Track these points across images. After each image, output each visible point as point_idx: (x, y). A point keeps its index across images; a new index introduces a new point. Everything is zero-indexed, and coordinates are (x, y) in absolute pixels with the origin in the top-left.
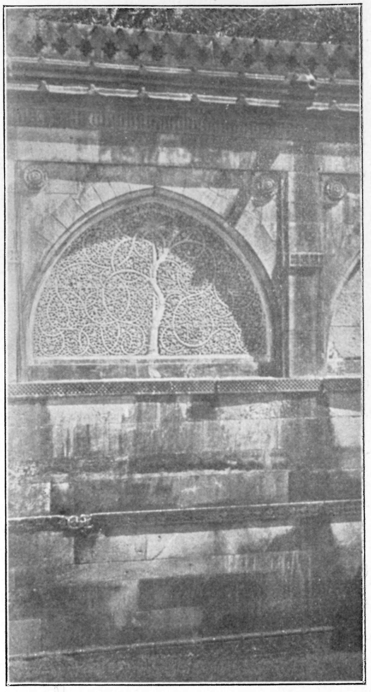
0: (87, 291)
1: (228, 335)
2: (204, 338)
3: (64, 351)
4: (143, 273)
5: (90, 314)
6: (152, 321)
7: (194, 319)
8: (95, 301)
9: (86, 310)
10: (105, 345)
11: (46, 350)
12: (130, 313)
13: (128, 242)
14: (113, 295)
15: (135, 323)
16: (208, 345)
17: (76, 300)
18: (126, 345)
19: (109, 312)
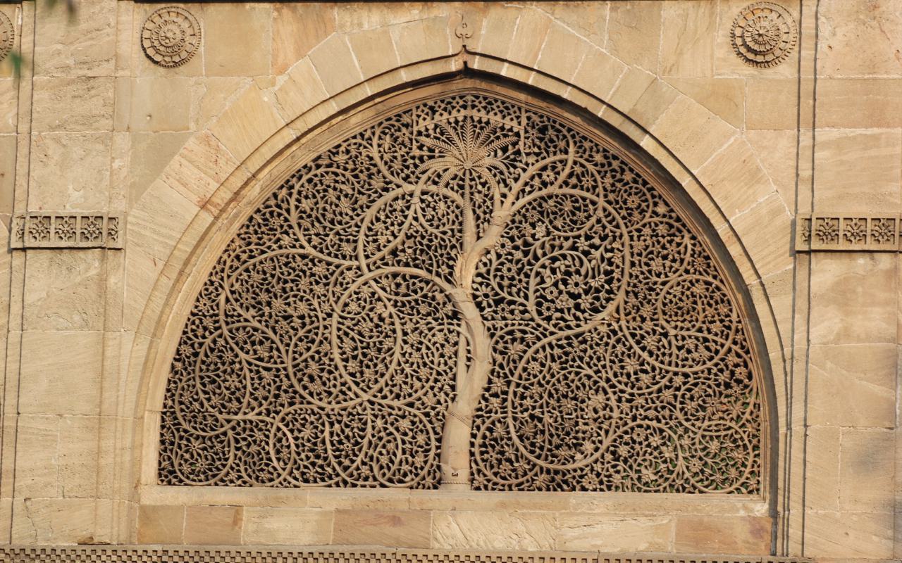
0: (297, 322)
1: (656, 440)
2: (588, 447)
3: (233, 475)
4: (438, 275)
5: (300, 380)
6: (453, 399)
8: (314, 348)
9: (291, 370)
10: (334, 461)
11: (186, 468)
12: (399, 379)
14: (360, 334)
15: (411, 405)
16: (598, 467)
17: (267, 344)
19: (348, 378)
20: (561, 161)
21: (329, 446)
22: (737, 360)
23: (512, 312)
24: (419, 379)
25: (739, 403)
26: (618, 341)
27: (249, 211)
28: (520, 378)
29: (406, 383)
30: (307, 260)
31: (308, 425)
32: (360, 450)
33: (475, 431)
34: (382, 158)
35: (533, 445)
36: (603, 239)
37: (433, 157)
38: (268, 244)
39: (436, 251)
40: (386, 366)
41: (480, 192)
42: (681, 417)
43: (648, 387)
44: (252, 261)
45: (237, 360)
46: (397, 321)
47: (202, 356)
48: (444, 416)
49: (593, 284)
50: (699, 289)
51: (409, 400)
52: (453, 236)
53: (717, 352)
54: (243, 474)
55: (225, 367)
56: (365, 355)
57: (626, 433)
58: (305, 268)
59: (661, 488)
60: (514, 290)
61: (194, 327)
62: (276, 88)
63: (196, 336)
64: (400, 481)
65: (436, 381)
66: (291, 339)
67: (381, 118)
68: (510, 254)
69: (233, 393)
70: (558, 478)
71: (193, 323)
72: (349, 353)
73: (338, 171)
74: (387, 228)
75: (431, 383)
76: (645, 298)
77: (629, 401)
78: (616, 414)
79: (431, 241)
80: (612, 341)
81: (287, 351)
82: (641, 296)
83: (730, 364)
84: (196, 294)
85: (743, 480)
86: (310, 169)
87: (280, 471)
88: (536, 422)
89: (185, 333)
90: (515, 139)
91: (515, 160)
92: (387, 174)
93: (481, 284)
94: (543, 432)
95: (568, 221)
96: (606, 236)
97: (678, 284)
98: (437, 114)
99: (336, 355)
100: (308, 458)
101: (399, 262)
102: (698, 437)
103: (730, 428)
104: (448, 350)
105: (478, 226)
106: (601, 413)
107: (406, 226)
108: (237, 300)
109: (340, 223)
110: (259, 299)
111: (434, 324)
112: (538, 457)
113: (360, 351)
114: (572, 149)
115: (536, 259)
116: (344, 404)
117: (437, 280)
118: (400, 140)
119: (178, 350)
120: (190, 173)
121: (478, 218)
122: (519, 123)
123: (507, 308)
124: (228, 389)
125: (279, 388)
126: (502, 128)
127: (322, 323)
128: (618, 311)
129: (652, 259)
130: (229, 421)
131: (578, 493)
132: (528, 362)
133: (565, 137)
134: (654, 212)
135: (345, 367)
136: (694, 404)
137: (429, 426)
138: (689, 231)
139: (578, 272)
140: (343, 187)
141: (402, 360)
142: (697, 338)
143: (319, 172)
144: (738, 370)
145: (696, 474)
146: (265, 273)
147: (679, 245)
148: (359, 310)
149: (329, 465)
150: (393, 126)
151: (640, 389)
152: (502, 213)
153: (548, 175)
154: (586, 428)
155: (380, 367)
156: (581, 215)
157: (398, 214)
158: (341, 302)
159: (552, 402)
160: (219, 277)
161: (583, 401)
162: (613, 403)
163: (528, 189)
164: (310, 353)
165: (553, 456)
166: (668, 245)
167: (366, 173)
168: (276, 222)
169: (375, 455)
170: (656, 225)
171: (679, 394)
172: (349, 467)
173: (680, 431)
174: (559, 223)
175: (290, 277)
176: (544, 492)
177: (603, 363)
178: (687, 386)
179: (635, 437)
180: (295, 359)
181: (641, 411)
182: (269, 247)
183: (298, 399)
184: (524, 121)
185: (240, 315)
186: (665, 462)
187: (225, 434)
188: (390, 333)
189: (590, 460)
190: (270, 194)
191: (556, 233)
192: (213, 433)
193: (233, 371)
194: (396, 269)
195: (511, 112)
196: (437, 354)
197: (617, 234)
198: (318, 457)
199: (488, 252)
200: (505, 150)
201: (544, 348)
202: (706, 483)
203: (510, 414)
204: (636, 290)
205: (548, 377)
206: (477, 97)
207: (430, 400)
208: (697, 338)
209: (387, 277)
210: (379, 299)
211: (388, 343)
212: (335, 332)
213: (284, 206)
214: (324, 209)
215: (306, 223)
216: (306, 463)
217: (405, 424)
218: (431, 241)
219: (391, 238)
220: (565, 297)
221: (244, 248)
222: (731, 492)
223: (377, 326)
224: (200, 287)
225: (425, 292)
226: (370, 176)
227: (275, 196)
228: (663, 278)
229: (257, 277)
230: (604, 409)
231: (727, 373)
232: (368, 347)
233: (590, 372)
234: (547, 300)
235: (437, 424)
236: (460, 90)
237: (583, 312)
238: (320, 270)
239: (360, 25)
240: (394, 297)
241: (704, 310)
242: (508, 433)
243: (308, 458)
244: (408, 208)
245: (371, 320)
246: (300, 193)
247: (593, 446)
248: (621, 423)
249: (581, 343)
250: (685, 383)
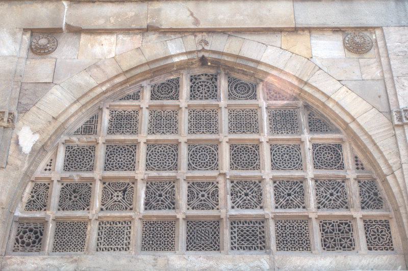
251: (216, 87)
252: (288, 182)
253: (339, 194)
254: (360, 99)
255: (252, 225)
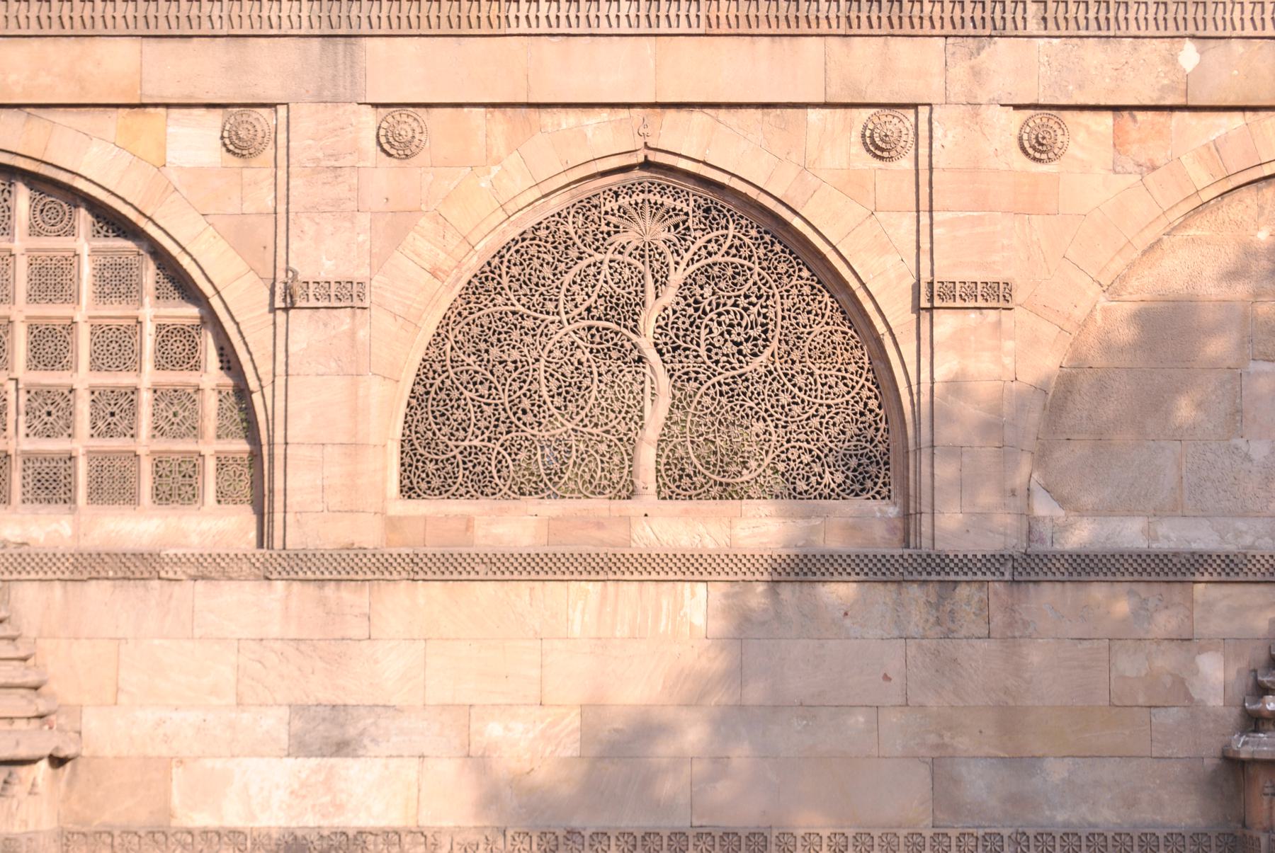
0: (511, 367)
1: (806, 458)
2: (753, 464)
3: (463, 490)
4: (625, 327)
5: (515, 414)
6: (641, 427)
7: (733, 424)
8: (526, 387)
9: (507, 406)
10: (546, 479)
11: (424, 485)
13: (595, 265)
14: (563, 375)
15: (607, 432)
17: (487, 384)
18: (587, 477)
20: (722, 236)
21: (541, 467)
22: (872, 394)
23: (687, 357)
24: (613, 411)
25: (872, 428)
26: (774, 379)
27: (468, 276)
28: (696, 409)
29: (602, 414)
30: (517, 316)
31: (523, 449)
32: (567, 468)
33: (660, 453)
34: (576, 233)
35: (708, 463)
36: (759, 297)
37: (618, 232)
38: (485, 303)
39: (623, 307)
40: (586, 401)
41: (657, 260)
42: (827, 440)
43: (799, 416)
44: (472, 317)
45: (463, 397)
46: (594, 365)
47: (433, 394)
48: (634, 441)
49: (751, 333)
50: (837, 338)
51: (605, 428)
52: (637, 295)
53: (853, 387)
54: (471, 489)
55: (453, 402)
56: (567, 392)
57: (783, 452)
58: (516, 322)
59: (812, 496)
60: (688, 339)
61: (425, 371)
62: (492, 176)
63: (427, 378)
64: (600, 493)
65: (627, 412)
66: (506, 379)
67: (575, 201)
68: (684, 310)
69: (460, 424)
70: (730, 489)
71: (425, 367)
72: (555, 391)
73: (541, 243)
74: (582, 290)
75: (623, 414)
76: (794, 345)
77: (783, 427)
78: (774, 438)
79: (618, 299)
80: (769, 380)
81: (503, 390)
82: (791, 343)
83: (864, 397)
84: (426, 344)
85: (877, 489)
86: (517, 242)
87: (502, 487)
88: (710, 444)
89: (418, 375)
90: (685, 217)
91: (685, 234)
92: (581, 246)
93: (661, 334)
94: (715, 453)
95: (730, 283)
96: (761, 296)
97: (821, 334)
98: (620, 197)
99: (544, 390)
100: (524, 476)
101: (593, 317)
102: (840, 455)
103: (865, 448)
104: (636, 388)
105: (657, 288)
106: (762, 437)
107: (598, 288)
108: (460, 349)
109: (544, 285)
110: (478, 347)
111: (624, 367)
112: (713, 472)
113: (563, 390)
114: (731, 226)
115: (705, 313)
116: (553, 432)
117: (624, 331)
118: (591, 218)
119: (412, 391)
120: (423, 245)
121: (656, 281)
122: (688, 205)
123: (683, 355)
124: (455, 420)
125: (497, 420)
126: (674, 209)
127: (531, 367)
128: (773, 355)
129: (799, 314)
130: (457, 447)
131: (745, 501)
132: (702, 396)
133: (725, 216)
134: (799, 276)
135: (552, 402)
136: (837, 429)
137: (623, 449)
138: (828, 291)
139: (739, 324)
140: (545, 256)
141: (599, 396)
142: (837, 377)
143: (525, 244)
144: (870, 402)
145: (839, 485)
146: (482, 326)
147: (820, 302)
148: (562, 355)
149: (541, 481)
150: (586, 207)
151: (792, 417)
152: (677, 277)
153: (713, 247)
154: (750, 449)
155: (581, 402)
156: (740, 279)
157: (591, 277)
158: (547, 350)
159: (722, 428)
160: (445, 329)
161: (747, 428)
162: (772, 429)
163: (696, 257)
164: (523, 391)
165: (724, 471)
166: (811, 303)
167: (564, 245)
168: (490, 285)
169: (580, 473)
170: (801, 286)
171: (824, 421)
172: (558, 483)
173: (826, 450)
174: (722, 285)
175: (505, 329)
176: (718, 501)
177: (762, 397)
178: (831, 415)
179: (790, 456)
180: (510, 396)
181: (794, 435)
182: (486, 306)
183: (514, 429)
184: (692, 203)
185: (463, 361)
186: (815, 475)
187: (454, 457)
188: (588, 374)
189: (754, 475)
190: (485, 262)
191: (721, 293)
192: (444, 457)
193: (459, 406)
194: (591, 322)
195: (681, 195)
196: (627, 391)
197: (771, 294)
198: (532, 474)
199: (666, 309)
200: (676, 226)
201: (714, 386)
202: (848, 491)
203: (689, 439)
204: (787, 338)
205: (718, 409)
206: (653, 184)
207: (622, 428)
208: (837, 377)
209: (584, 329)
210: (578, 347)
211: (587, 382)
212: (543, 374)
213: (497, 271)
214: (530, 274)
215: (515, 286)
216: (523, 480)
217: (603, 448)
218: (618, 299)
219: (586, 298)
220: (729, 344)
221: (464, 306)
222: (869, 499)
223: (577, 369)
224: (429, 338)
225: (615, 341)
226: (566, 248)
227: (489, 264)
228: (808, 329)
229: (476, 331)
230: (764, 433)
231: (862, 404)
232: (570, 385)
233: (752, 404)
234: (715, 347)
235: (629, 447)
236: (639, 178)
237: (745, 356)
238: (528, 323)
239: (559, 125)
240: (590, 346)
241: (842, 354)
242: (687, 453)
243: (524, 476)
244: (599, 273)
245: (572, 364)
246: (509, 261)
247: (756, 463)
248: (778, 444)
249: (743, 381)
250: (828, 413)
251: (9, 209)
252: (113, 392)
253: (187, 414)
254: (232, 253)
255: (54, 464)
